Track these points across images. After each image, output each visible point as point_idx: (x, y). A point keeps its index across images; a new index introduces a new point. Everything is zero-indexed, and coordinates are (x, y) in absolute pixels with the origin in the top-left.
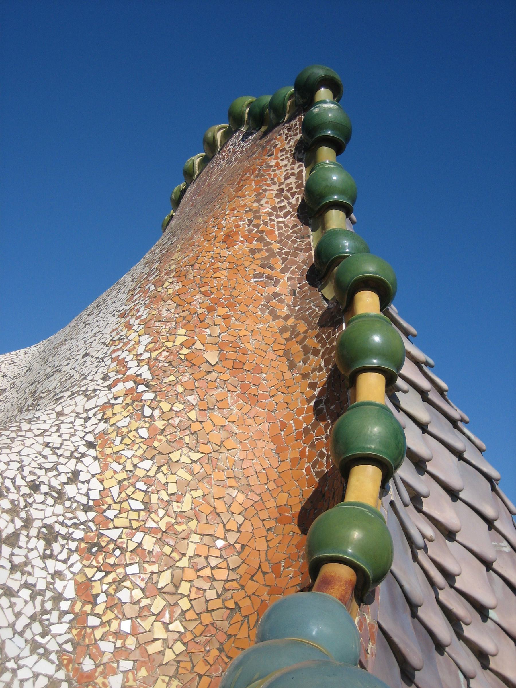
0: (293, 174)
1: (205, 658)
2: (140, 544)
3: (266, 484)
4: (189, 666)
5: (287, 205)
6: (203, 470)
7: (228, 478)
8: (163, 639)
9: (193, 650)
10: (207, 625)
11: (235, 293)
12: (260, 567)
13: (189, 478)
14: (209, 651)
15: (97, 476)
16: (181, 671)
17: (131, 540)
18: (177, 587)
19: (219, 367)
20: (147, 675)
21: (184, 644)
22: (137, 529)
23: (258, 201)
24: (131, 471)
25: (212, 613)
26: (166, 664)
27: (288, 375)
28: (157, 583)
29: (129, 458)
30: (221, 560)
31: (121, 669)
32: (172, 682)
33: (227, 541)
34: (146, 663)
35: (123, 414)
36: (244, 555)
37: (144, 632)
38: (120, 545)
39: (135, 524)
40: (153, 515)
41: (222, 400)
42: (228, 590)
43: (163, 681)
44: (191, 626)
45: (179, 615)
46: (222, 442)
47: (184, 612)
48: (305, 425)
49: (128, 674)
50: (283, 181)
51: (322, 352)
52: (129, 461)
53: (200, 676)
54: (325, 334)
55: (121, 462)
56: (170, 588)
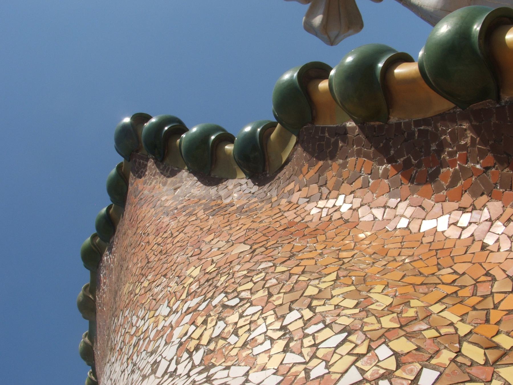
2: (396, 354)
15: (250, 372)
17: (379, 361)
18: (497, 347)
22: (370, 349)
24: (284, 335)
28: (473, 363)
29: (266, 332)
30: (490, 298)
35: (208, 328)
38: (377, 376)
39: (362, 349)
40: (365, 329)
41: (293, 248)
46: (338, 258)
52: (270, 333)
55: (261, 342)
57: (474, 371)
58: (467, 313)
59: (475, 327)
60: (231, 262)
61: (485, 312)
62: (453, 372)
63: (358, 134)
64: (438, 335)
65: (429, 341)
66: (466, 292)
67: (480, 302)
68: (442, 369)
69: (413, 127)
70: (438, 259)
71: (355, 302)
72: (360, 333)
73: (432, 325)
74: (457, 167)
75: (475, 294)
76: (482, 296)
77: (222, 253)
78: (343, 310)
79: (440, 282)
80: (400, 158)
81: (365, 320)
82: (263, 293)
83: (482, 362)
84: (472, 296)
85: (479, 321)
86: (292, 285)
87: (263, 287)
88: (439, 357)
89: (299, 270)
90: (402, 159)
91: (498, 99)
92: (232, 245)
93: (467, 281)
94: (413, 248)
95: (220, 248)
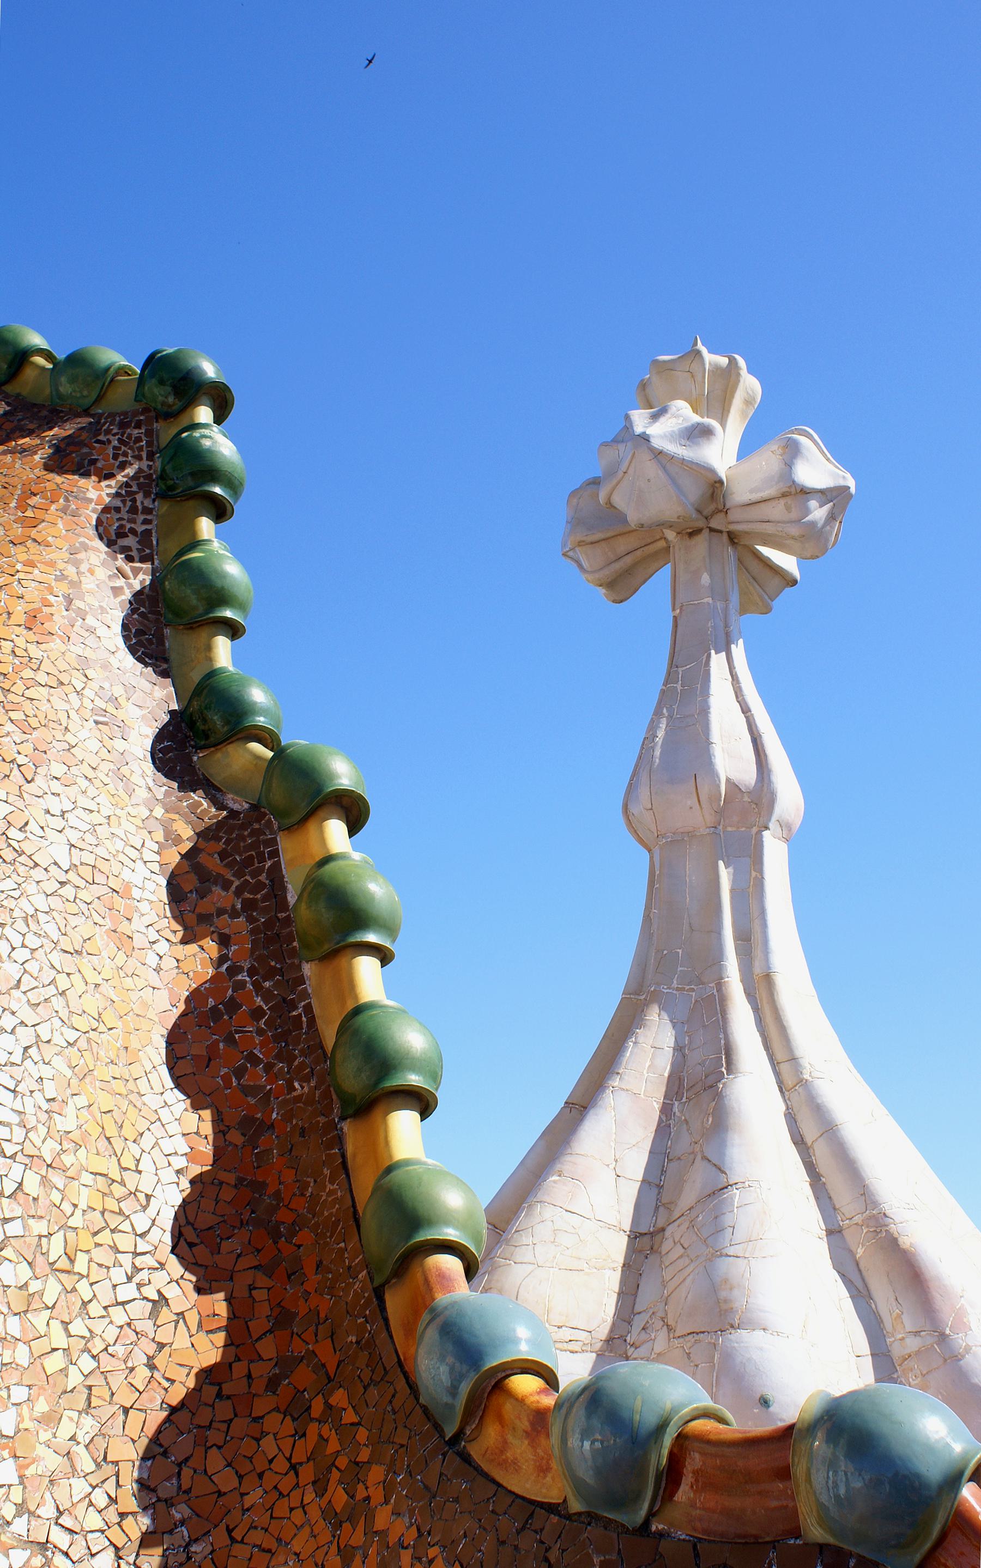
0: (133, 531)
1: (129, 1380)
5: (125, 588)
6: (82, 1061)
8: (64, 1349)
10: (121, 1327)
11: (69, 737)
13: (69, 1073)
14: (132, 1369)
17: (6, 1176)
18: (72, 1261)
19: (72, 876)
20: (47, 1409)
21: (94, 1357)
23: (77, 564)
25: (126, 1307)
26: (72, 1391)
30: (122, 1218)
31: (13, 1400)
36: (152, 1211)
41: (89, 939)
43: (71, 1419)
46: (100, 1014)
47: (85, 1304)
48: (211, 1003)
50: (114, 537)
51: (234, 886)
54: (241, 855)
56: (63, 1263)
57: (40, 1259)
58: (95, 1210)
62: (29, 1246)
65: (48, 1202)
66: (118, 1190)
67: (113, 1212)
68: (27, 1234)
69: (303, 1004)
70: (148, 1129)
74: (268, 1087)
76: (120, 1209)
80: (263, 999)
81: (40, 1126)
83: (51, 1261)
91: (343, 1118)
94: (152, 1088)
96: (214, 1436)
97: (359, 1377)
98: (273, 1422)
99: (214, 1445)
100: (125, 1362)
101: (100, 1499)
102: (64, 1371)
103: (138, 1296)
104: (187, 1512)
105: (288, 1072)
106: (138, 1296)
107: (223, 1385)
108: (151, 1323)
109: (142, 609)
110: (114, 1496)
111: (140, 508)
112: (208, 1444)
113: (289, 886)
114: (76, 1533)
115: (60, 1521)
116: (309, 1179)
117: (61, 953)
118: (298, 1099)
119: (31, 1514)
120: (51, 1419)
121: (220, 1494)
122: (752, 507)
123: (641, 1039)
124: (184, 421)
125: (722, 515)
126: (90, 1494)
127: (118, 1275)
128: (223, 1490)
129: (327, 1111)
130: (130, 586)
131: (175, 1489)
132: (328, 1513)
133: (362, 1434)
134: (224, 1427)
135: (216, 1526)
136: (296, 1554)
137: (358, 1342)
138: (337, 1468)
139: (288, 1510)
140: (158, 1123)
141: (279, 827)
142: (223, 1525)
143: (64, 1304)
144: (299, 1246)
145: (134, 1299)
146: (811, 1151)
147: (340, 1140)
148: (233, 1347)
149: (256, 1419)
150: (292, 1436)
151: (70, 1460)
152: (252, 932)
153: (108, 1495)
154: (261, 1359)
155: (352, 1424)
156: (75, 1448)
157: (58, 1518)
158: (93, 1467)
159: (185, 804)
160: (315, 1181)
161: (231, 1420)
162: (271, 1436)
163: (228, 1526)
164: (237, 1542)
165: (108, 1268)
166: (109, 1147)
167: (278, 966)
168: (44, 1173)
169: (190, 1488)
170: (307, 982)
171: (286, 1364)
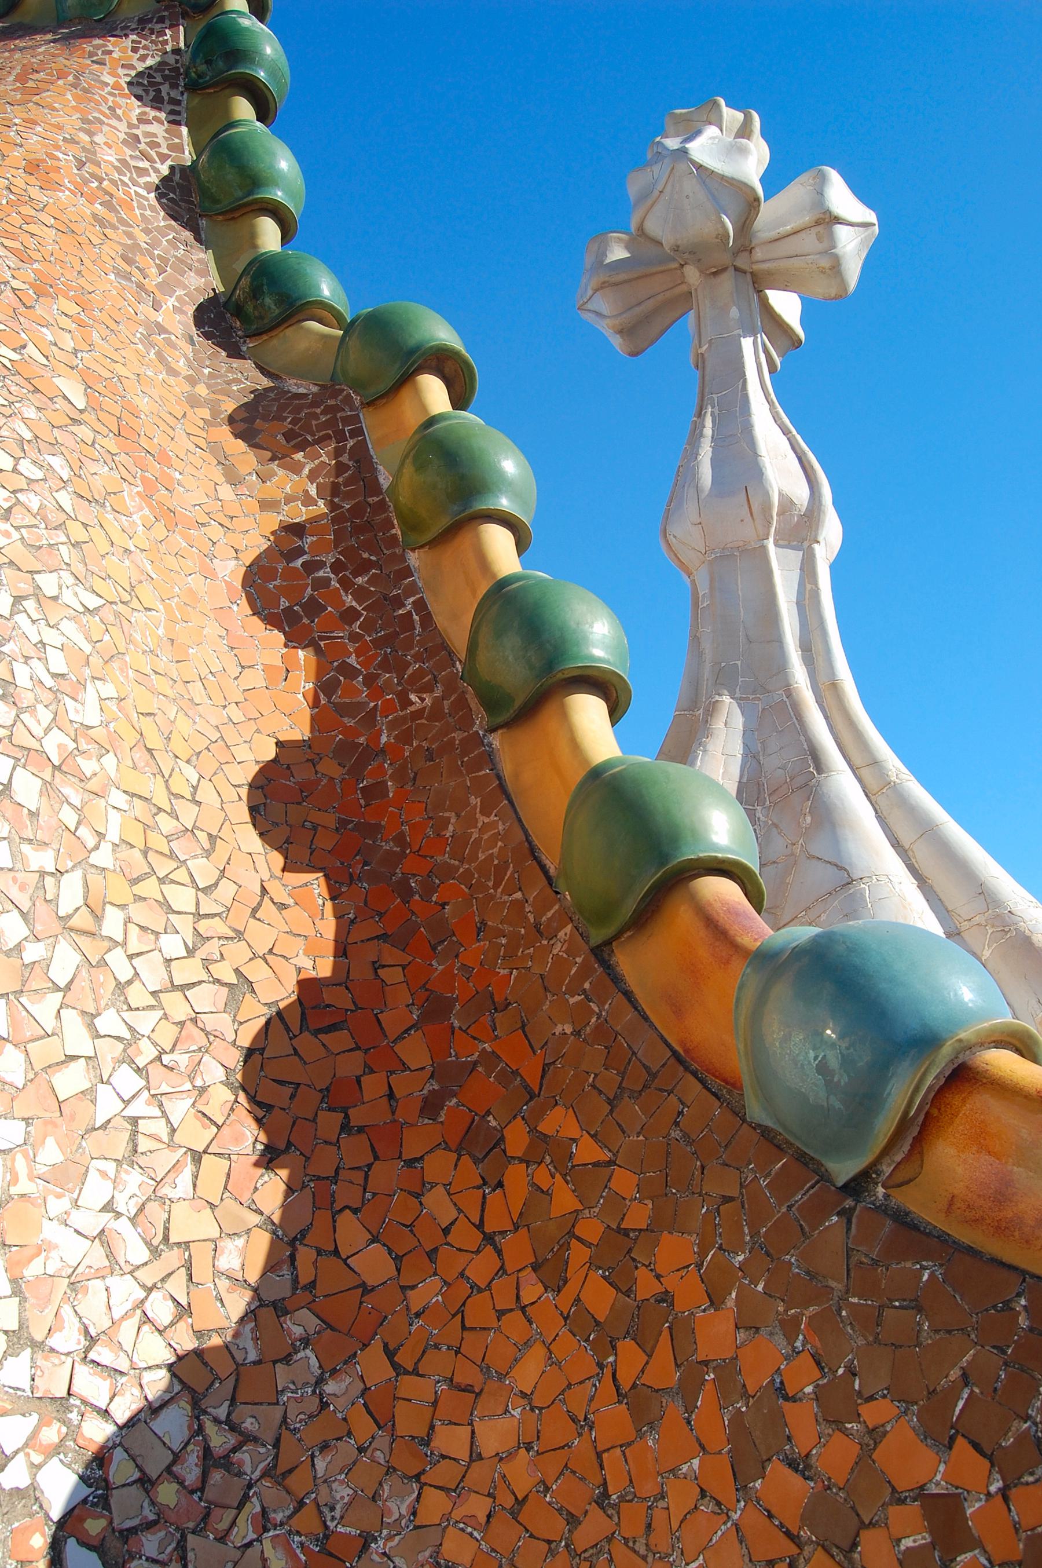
3: (225, 706)
4: (160, 1128)
7: (156, 673)
9: (165, 1088)
10: (182, 1024)
12: (264, 891)
13: (87, 648)
14: (203, 1090)
16: (144, 1144)
20: (62, 1158)
21: (138, 1070)
26: (104, 1126)
27: (226, 492)
28: (54, 902)
32: (123, 1175)
33: (178, 819)
34: (55, 1125)
37: (42, 1038)
41: (115, 493)
42: (209, 939)
43: (104, 1174)
44: (145, 1022)
45: (113, 994)
47: (121, 987)
48: (284, 603)
49: (13, 1160)
53: (197, 1157)
58: (132, 846)
59: (114, 871)
60: (36, 390)
61: (148, 870)
63: (370, 505)
64: (73, 830)
65: (54, 822)
66: (167, 825)
68: (19, 866)
69: (411, 600)
70: (207, 748)
71: (63, 670)
72: (14, 712)
73: (85, 810)
74: (372, 704)
75: (170, 838)
76: (171, 851)
77: (47, 358)
78: (39, 659)
79: (167, 777)
80: (355, 598)
81: (40, 707)
82: (5, 500)
83: (62, 913)
84: (166, 837)
85: (127, 871)
86: (45, 542)
87: (14, 492)
88: (36, 850)
89: (77, 532)
90: (354, 604)
91: (493, 730)
92: (72, 368)
93: (188, 814)
95: (56, 344)
96: (345, 1193)
97: (593, 1086)
98: (439, 1165)
99: (347, 1207)
100: (191, 1079)
101: (161, 1310)
102: (89, 1095)
103: (205, 977)
104: (313, 1323)
105: (399, 683)
106: (205, 977)
107: (351, 1112)
108: (227, 1018)
109: (172, 195)
110: (184, 1303)
111: (166, 98)
112: (337, 1206)
113: (381, 468)
114: (121, 1373)
115: (92, 1355)
116: (447, 814)
117: (74, 496)
118: (419, 714)
119: (37, 1346)
120: (68, 1177)
121: (366, 1289)
122: (778, 243)
123: (710, 747)
124: (215, 11)
125: (746, 254)
126: (142, 1302)
127: (173, 945)
128: (370, 1282)
129: (467, 721)
130: (157, 171)
131: (289, 1285)
132: (578, 1319)
133: (624, 1181)
134: (358, 1177)
135: (365, 1346)
136: (523, 1395)
137: (577, 1033)
138: (579, 1239)
139: (493, 1315)
140: (221, 742)
141: (362, 403)
142: (377, 1344)
143: (86, 984)
144: (443, 906)
145: (200, 982)
146: (910, 853)
147: (489, 758)
148: (359, 1054)
149: (410, 1163)
150: (478, 1187)
151: (107, 1246)
152: (334, 521)
153: (174, 1300)
154: (405, 1067)
155: (596, 1164)
156: (115, 1225)
157: (87, 1350)
158: (144, 1255)
159: (235, 388)
160: (458, 816)
161: (370, 1166)
162: (440, 1188)
163: (386, 1346)
164: (407, 1373)
165: (157, 934)
166: (151, 761)
167: (373, 558)
168: (48, 778)
169: (314, 1282)
170: (415, 574)
171: (450, 1077)
